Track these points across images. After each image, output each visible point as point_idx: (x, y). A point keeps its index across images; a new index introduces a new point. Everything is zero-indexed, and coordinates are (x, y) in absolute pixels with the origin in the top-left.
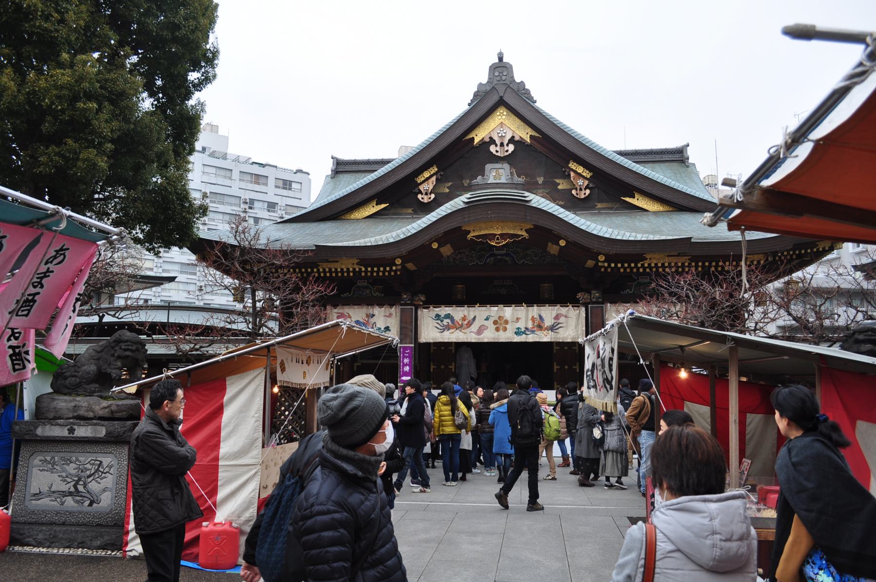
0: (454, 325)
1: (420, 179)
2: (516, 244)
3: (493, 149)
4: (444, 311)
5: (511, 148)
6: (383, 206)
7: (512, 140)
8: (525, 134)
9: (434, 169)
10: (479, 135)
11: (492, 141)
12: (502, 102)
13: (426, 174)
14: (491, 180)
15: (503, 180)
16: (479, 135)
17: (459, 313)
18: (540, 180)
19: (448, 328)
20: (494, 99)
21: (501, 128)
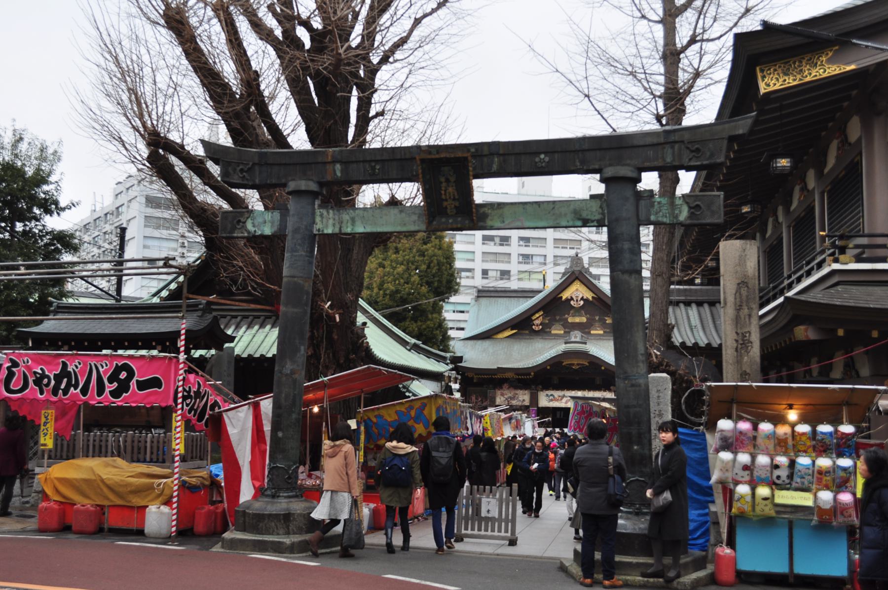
0: (555, 399)
1: (534, 318)
2: (583, 368)
3: (572, 303)
4: (550, 392)
5: (582, 303)
6: (514, 331)
7: (582, 299)
8: (589, 295)
9: (541, 313)
10: (565, 295)
11: (572, 299)
12: (577, 278)
13: (537, 315)
14: (573, 339)
15: (578, 340)
16: (565, 295)
17: (557, 393)
18: (597, 318)
19: (552, 400)
20: (574, 277)
21: (577, 292)
